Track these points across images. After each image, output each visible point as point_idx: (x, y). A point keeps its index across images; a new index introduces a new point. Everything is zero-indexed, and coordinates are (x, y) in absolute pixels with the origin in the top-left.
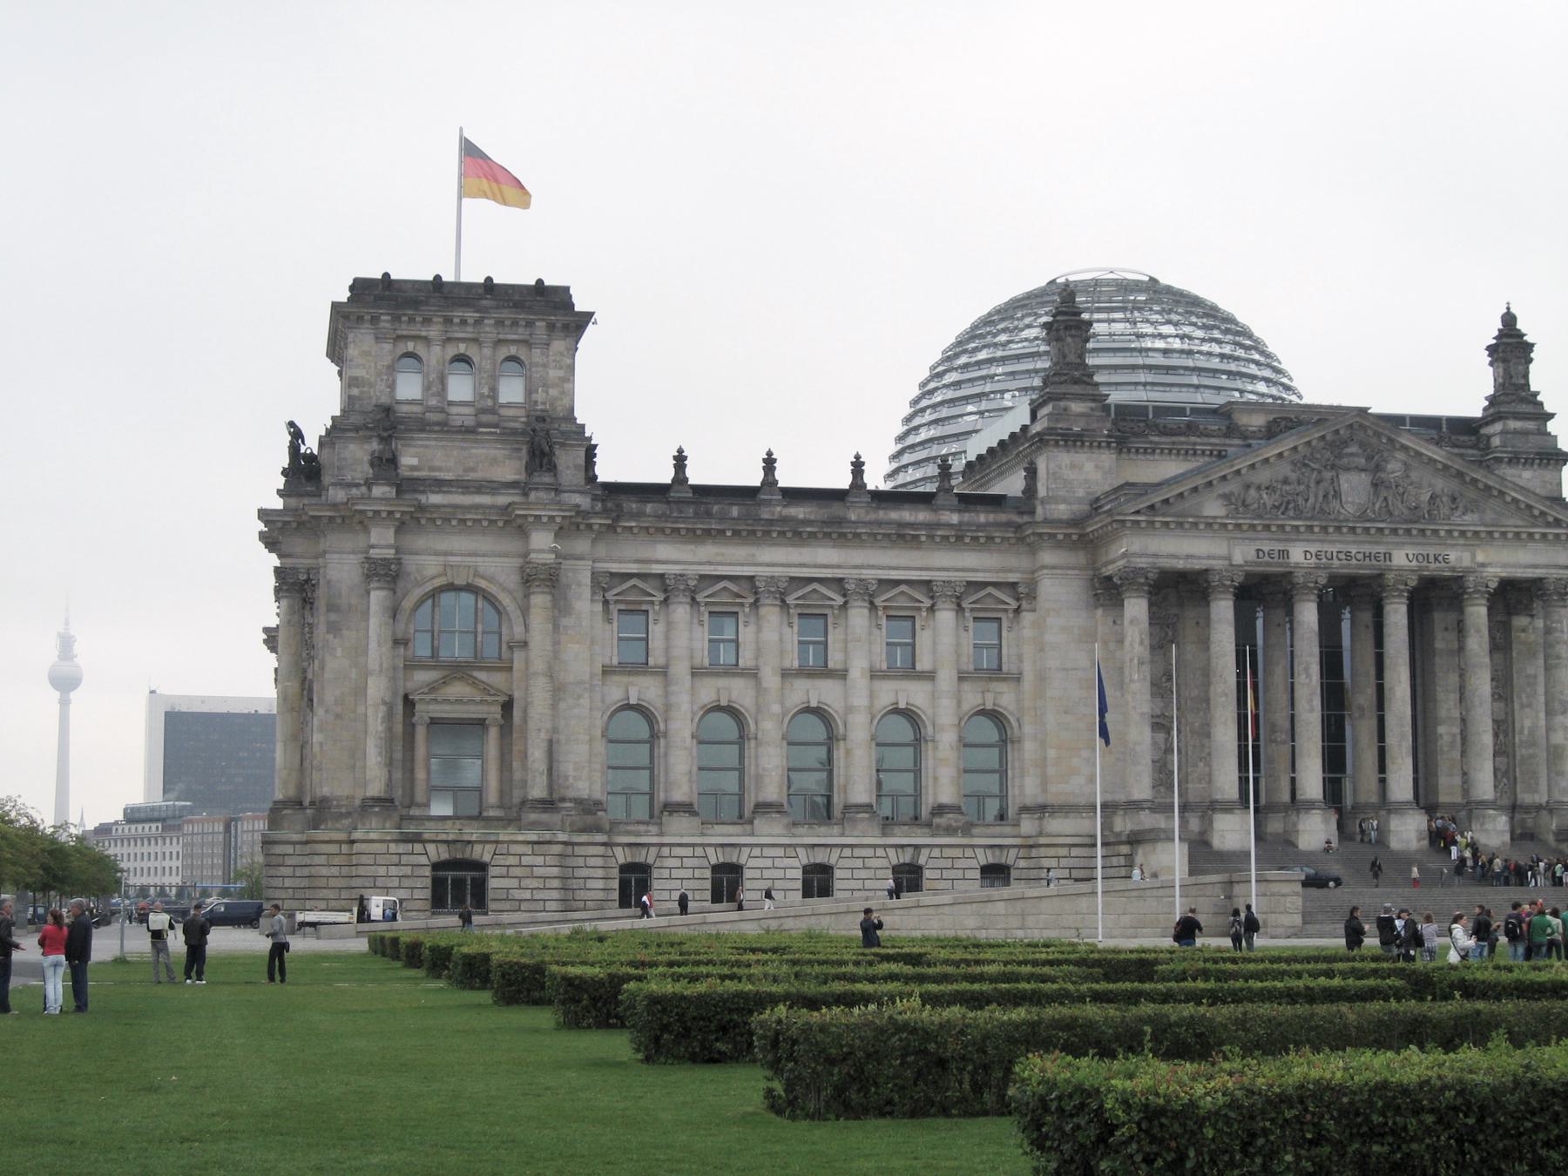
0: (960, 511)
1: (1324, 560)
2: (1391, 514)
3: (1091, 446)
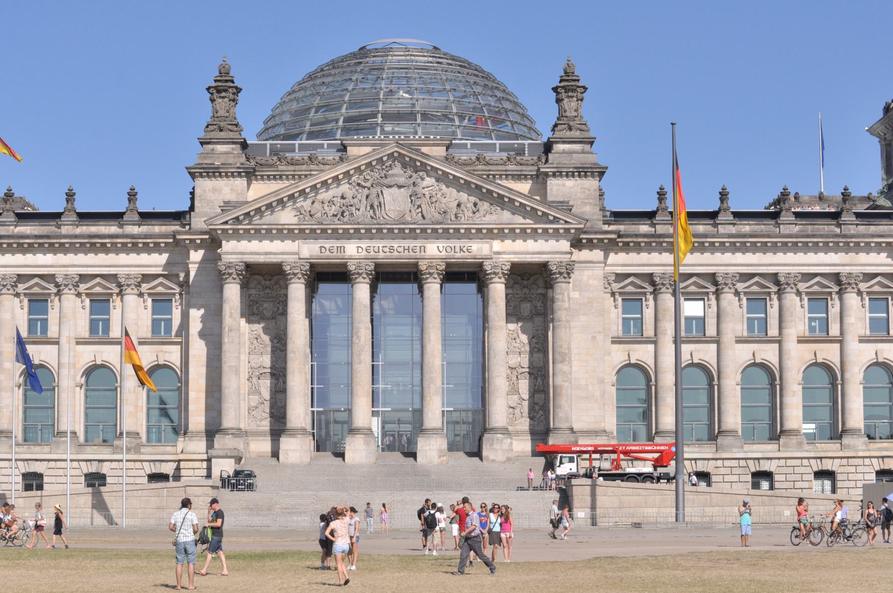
0: (139, 225)
1: (373, 253)
2: (423, 217)
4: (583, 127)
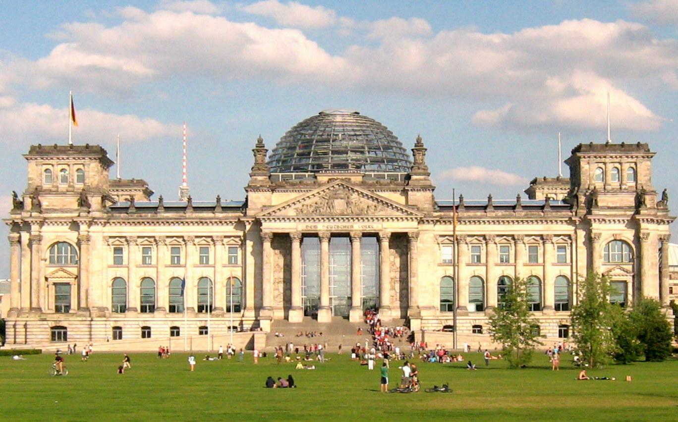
0: (222, 213)
2: (352, 212)
3: (262, 190)
4: (425, 168)
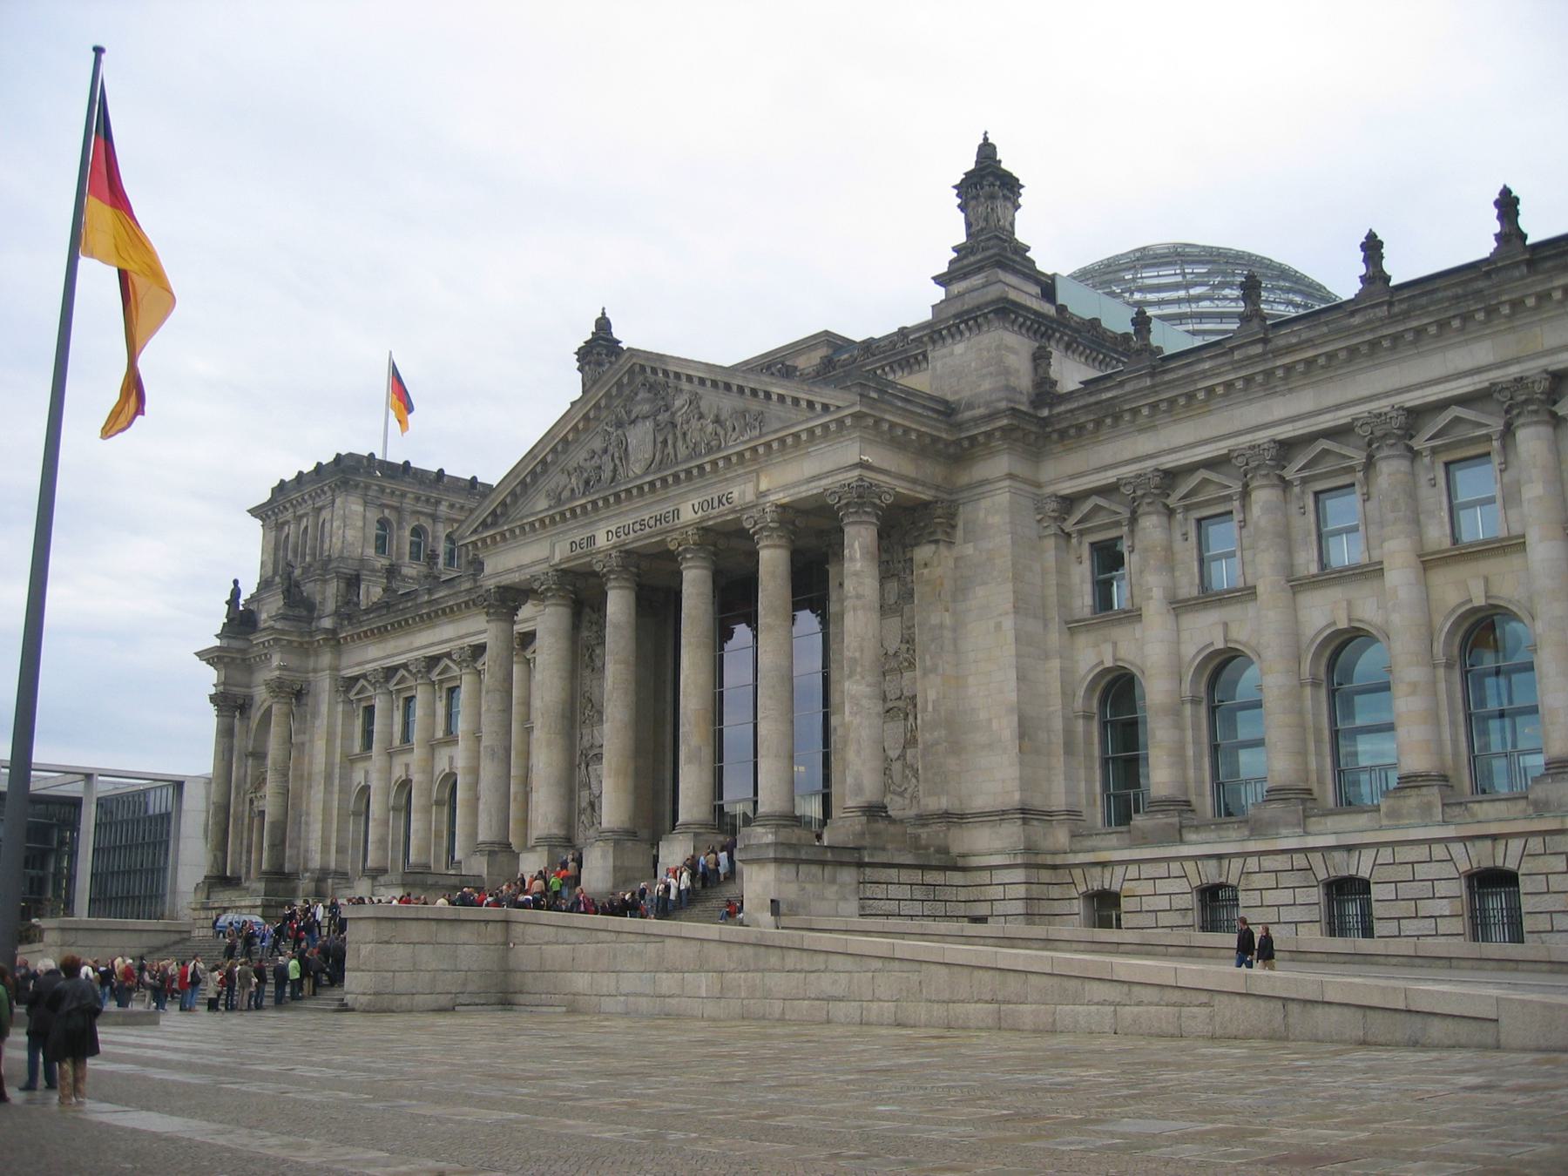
1: (623, 537)
